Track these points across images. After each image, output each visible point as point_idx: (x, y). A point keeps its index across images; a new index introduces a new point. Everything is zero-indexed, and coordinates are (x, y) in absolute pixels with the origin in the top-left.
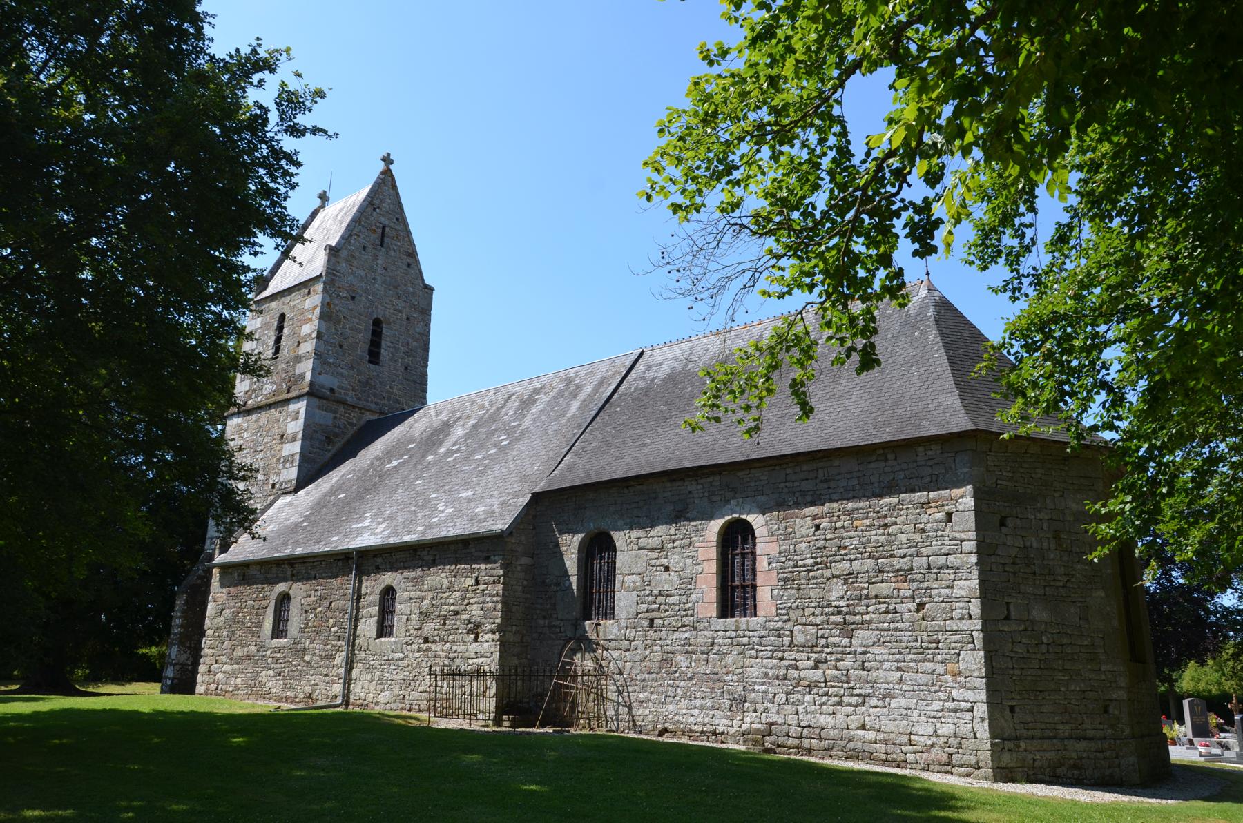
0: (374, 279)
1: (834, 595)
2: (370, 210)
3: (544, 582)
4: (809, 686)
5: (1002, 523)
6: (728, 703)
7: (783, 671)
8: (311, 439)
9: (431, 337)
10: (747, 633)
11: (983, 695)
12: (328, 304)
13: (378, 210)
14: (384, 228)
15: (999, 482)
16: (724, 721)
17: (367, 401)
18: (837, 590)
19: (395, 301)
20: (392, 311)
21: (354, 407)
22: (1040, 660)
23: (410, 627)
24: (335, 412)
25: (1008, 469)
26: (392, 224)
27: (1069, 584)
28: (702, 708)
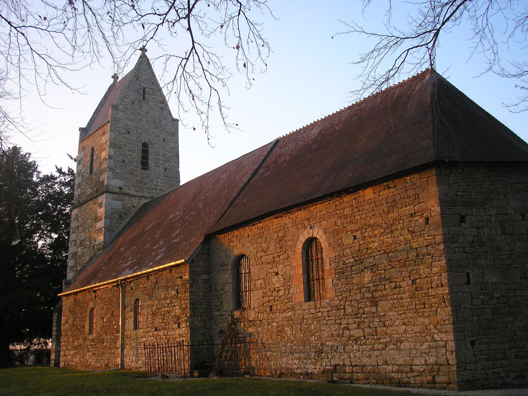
0: (141, 120)
1: (366, 280)
3: (216, 289)
4: (355, 339)
5: (463, 219)
6: (313, 354)
7: (341, 332)
8: (110, 218)
9: (179, 149)
10: (321, 309)
11: (451, 336)
15: (458, 193)
16: (312, 366)
18: (367, 276)
20: (153, 137)
22: (492, 309)
23: (148, 322)
24: (124, 200)
25: (464, 184)
27: (512, 256)
28: (299, 359)
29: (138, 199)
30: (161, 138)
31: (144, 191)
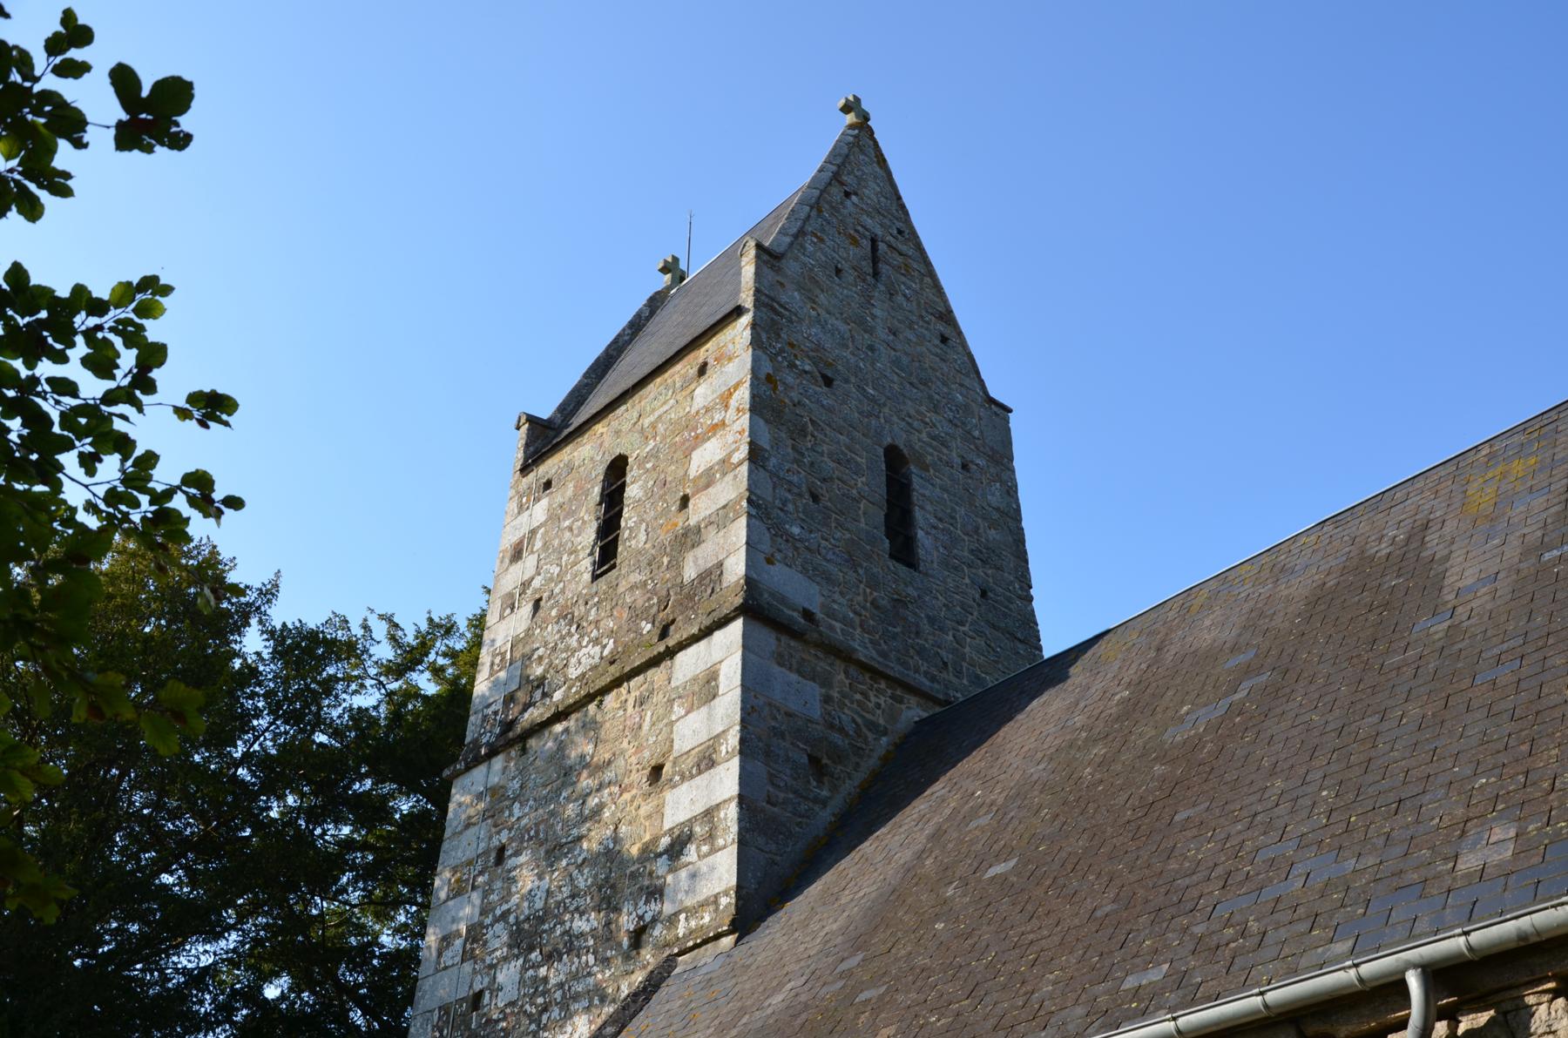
2: (836, 193)
8: (768, 754)
9: (1024, 524)
12: (769, 378)
13: (854, 198)
14: (874, 241)
17: (904, 664)
19: (931, 417)
21: (876, 674)
24: (826, 682)
26: (889, 238)
29: (889, 691)
30: (954, 454)
31: (911, 661)
